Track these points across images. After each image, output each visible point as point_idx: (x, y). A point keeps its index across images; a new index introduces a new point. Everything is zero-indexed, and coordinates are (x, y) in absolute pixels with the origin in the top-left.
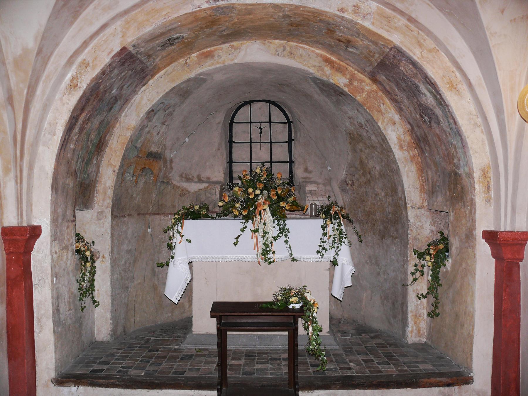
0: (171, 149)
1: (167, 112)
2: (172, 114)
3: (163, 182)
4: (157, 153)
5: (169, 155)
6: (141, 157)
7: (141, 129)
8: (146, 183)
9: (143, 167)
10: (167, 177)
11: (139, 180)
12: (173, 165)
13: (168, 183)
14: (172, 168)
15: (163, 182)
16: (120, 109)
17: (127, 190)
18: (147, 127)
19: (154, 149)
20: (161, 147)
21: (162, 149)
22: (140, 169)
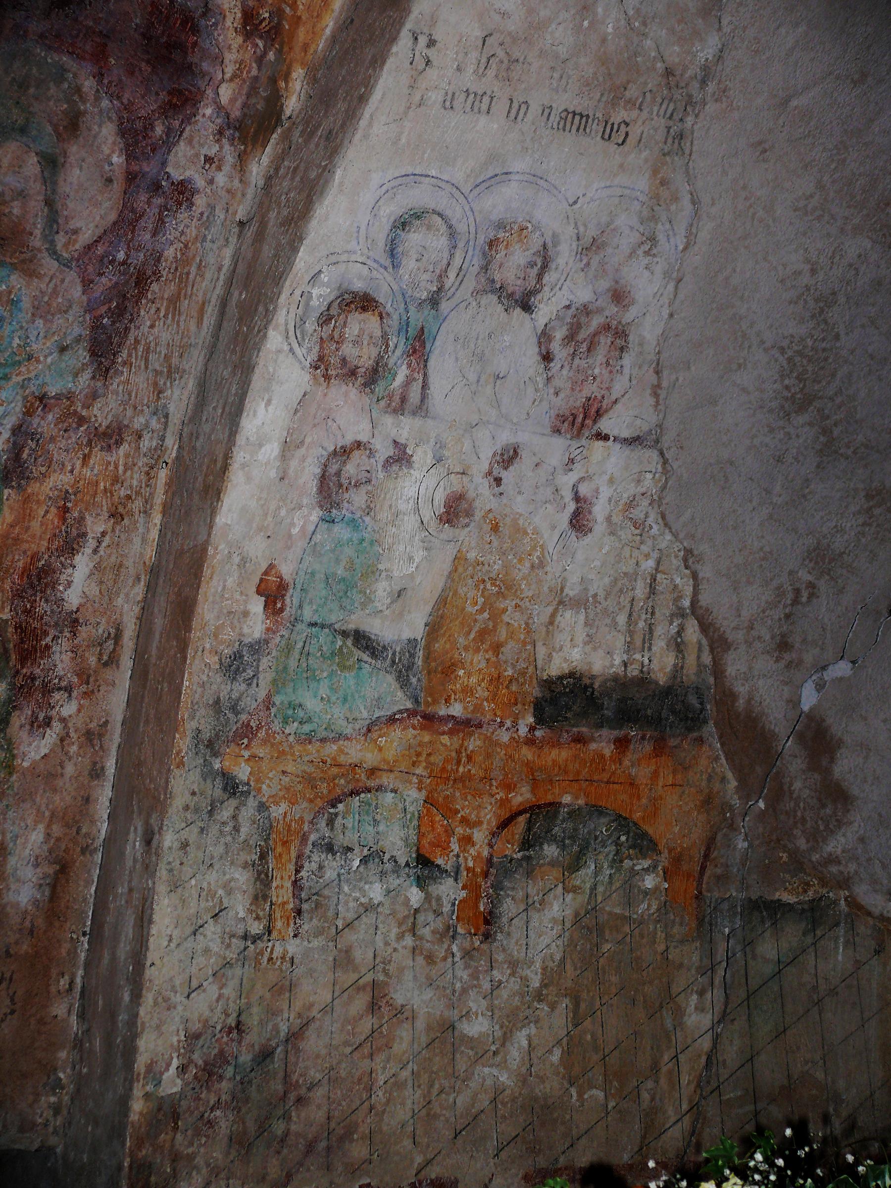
0: (784, 645)
1: (547, 309)
2: (619, 334)
3: (766, 911)
4: (643, 681)
5: (757, 682)
6: (464, 726)
7: (330, 489)
8: (588, 926)
9: (522, 796)
10: (798, 863)
11: (509, 907)
12: (844, 766)
13: (815, 914)
14: (837, 796)
15: (766, 911)
16: (104, 350)
17: (377, 997)
18: (400, 457)
19: (581, 649)
20: (664, 631)
21: (678, 645)
22: (489, 815)
